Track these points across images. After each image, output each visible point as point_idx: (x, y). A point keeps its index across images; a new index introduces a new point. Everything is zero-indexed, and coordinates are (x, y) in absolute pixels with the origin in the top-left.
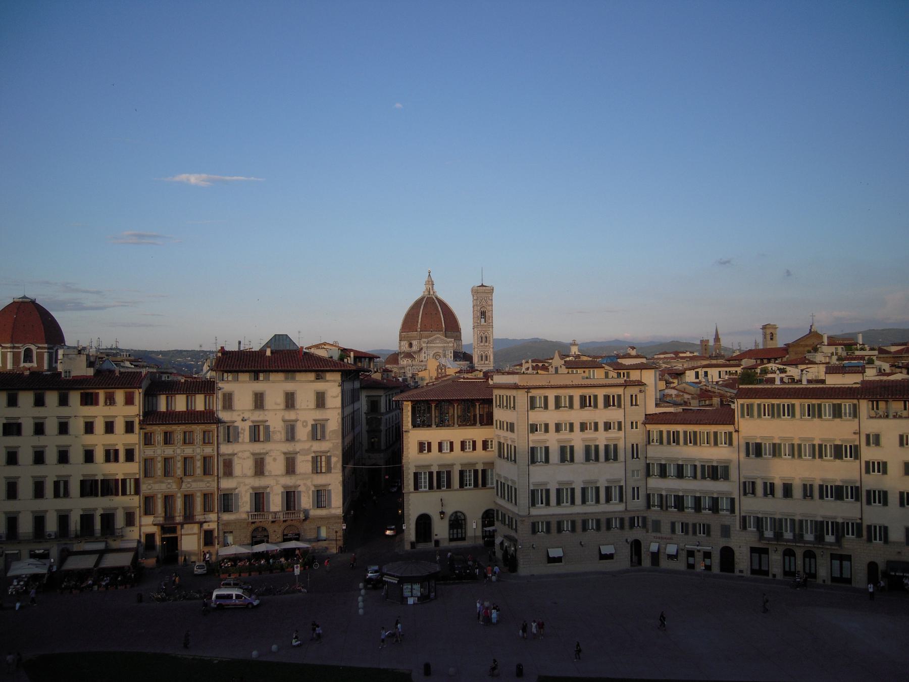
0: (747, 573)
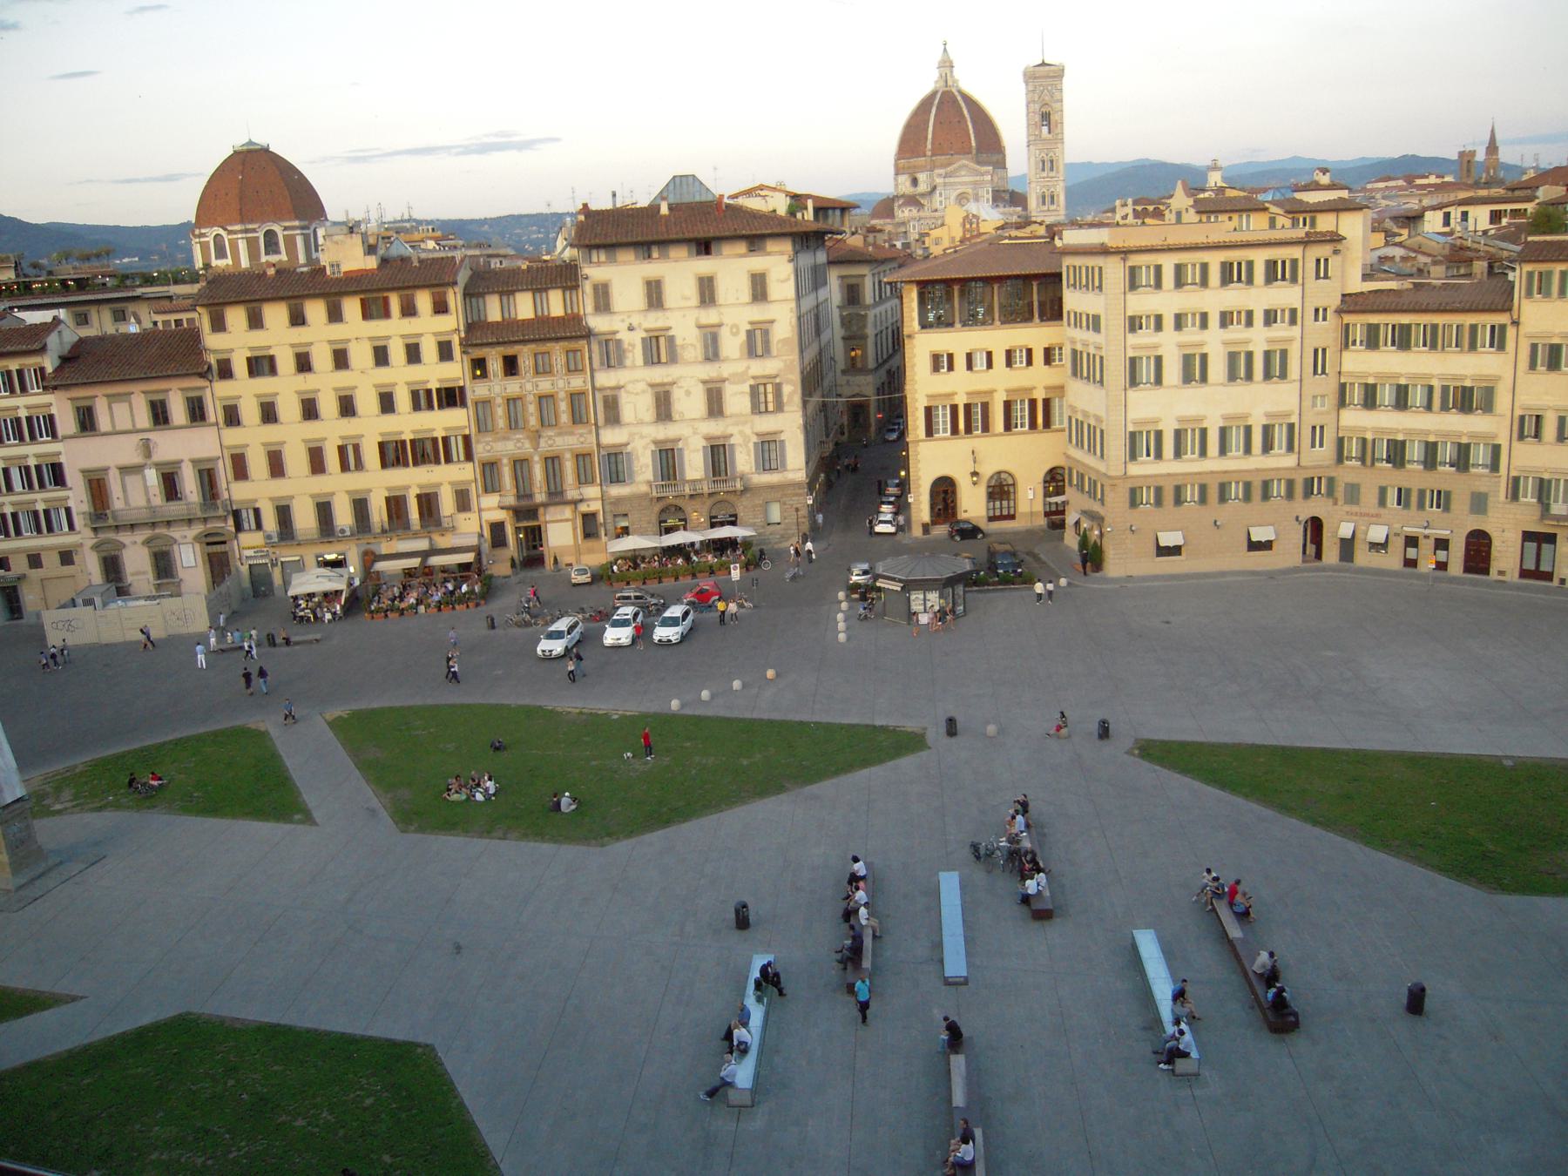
0: (1513, 576)
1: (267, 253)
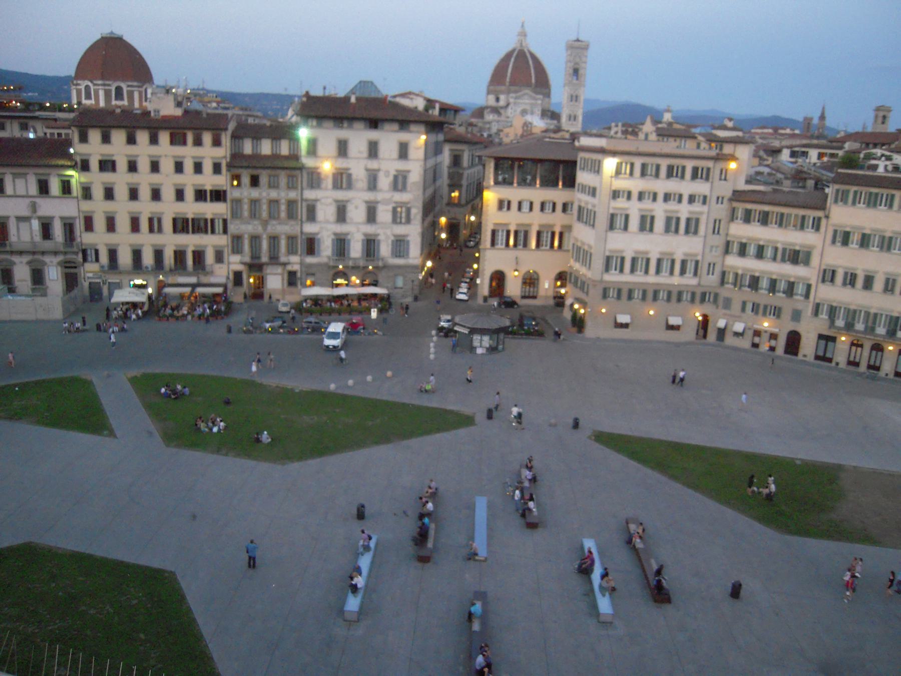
0: (811, 358)
1: (116, 99)
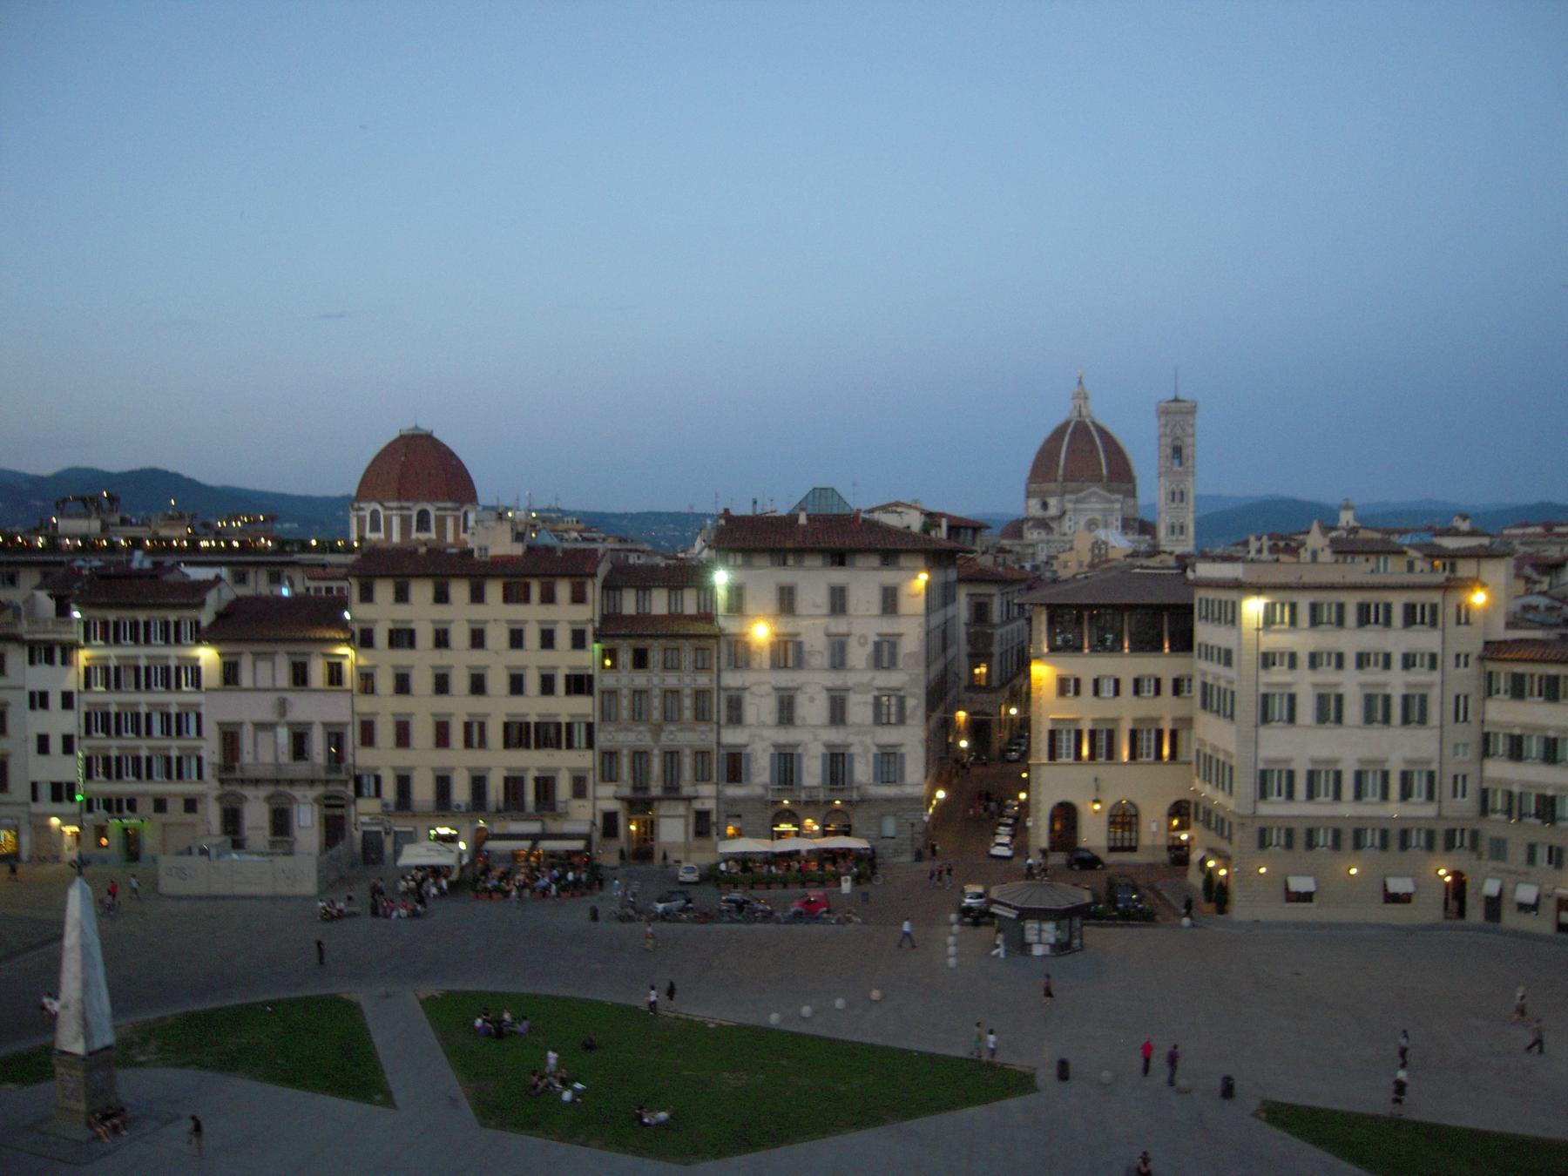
1: (419, 529)
